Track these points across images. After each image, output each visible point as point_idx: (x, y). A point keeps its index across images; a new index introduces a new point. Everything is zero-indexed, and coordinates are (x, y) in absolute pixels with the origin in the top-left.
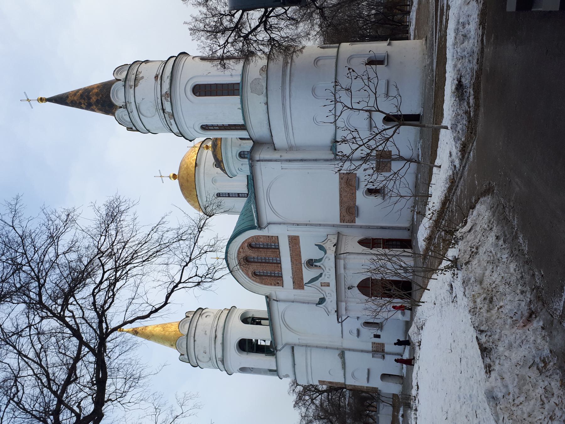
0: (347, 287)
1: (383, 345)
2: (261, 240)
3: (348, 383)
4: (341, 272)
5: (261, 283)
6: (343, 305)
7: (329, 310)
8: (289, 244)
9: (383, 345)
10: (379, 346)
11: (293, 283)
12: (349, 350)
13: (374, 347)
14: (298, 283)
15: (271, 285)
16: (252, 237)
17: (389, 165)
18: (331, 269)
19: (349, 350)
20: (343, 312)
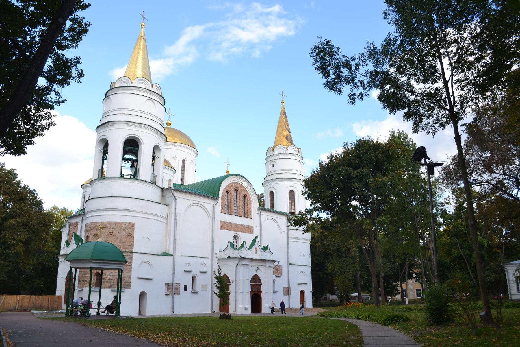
0: (259, 267)
1: (179, 294)
2: (249, 206)
3: (134, 256)
4: (267, 264)
5: (222, 195)
6: (248, 263)
7: (242, 251)
8: (248, 226)
9: (179, 294)
10: (178, 290)
11: (224, 222)
12: (174, 262)
13: (176, 286)
14: (225, 226)
15: (221, 203)
16: (250, 200)
17: (286, 294)
18: (265, 257)
19: (174, 262)
20: (244, 262)
